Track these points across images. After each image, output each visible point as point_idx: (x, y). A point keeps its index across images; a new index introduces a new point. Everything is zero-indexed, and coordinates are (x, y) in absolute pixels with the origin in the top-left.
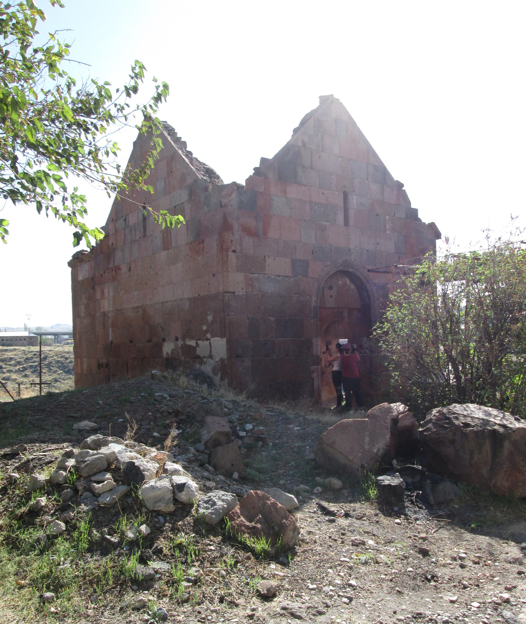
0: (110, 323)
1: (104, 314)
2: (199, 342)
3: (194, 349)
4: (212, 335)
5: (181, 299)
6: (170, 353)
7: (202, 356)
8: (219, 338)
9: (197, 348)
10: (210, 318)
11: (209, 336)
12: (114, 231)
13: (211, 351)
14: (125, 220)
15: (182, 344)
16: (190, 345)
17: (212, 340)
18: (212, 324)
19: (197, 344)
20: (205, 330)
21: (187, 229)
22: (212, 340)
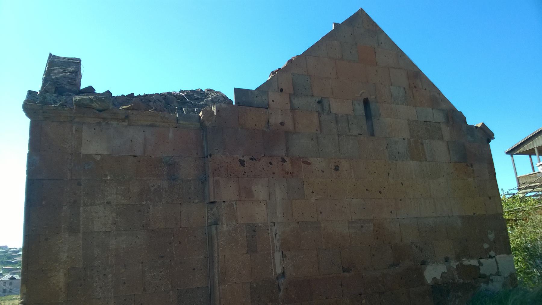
1: (253, 229)
2: (482, 260)
5: (449, 216)
6: (438, 277)
7: (488, 274)
8: (505, 255)
9: (481, 267)
10: (491, 236)
11: (492, 253)
12: (289, 108)
13: (498, 269)
14: (319, 102)
15: (457, 266)
17: (497, 257)
18: (494, 242)
19: (479, 262)
20: (487, 249)
21: (448, 149)
22: (497, 257)
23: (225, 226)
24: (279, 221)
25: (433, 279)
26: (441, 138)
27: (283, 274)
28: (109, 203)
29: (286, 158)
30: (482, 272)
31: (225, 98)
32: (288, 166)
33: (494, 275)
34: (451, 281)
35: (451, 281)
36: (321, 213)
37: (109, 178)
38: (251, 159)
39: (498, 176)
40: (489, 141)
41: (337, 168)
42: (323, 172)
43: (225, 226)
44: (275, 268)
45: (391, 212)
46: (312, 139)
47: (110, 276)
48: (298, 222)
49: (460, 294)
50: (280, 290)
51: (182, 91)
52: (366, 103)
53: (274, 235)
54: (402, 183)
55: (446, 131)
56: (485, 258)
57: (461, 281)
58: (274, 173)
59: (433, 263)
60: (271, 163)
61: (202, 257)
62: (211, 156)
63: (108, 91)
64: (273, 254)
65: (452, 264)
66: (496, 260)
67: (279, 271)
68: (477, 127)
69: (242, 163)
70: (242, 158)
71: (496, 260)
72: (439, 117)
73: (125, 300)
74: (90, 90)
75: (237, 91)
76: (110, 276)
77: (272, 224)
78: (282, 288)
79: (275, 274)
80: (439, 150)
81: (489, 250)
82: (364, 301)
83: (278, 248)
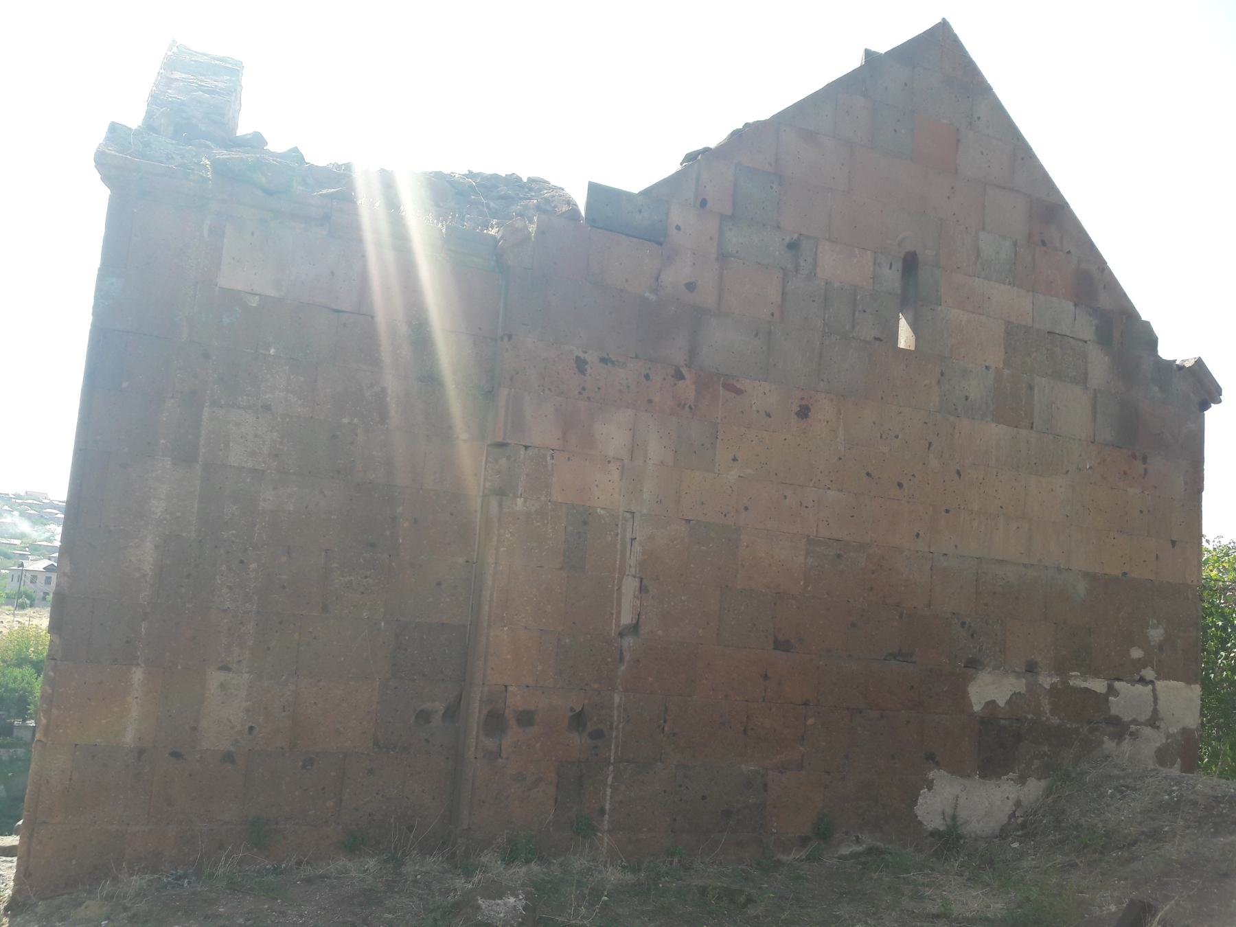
0: (632, 560)
2: (1117, 684)
3: (1101, 701)
4: (1157, 672)
5: (1058, 569)
7: (1126, 719)
8: (1181, 684)
9: (1111, 699)
10: (1156, 634)
11: (1149, 673)
13: (1155, 711)
14: (793, 246)
16: (1087, 690)
17: (1160, 684)
18: (1161, 648)
19: (1111, 690)
23: (520, 501)
24: (645, 511)
25: (988, 703)
26: (1083, 380)
27: (635, 628)
28: (267, 408)
29: (684, 371)
30: (1114, 711)
31: (569, 202)
32: (687, 389)
33: (1141, 724)
34: (1029, 717)
35: (1029, 717)
36: (746, 509)
37: (272, 351)
38: (604, 360)
39: (1206, 496)
40: (1205, 406)
41: (804, 412)
42: (769, 416)
43: (520, 501)
44: (619, 613)
45: (918, 535)
46: (757, 335)
47: (253, 566)
48: (689, 521)
49: (1046, 749)
50: (621, 659)
51: (471, 175)
52: (910, 264)
53: (628, 540)
54: (958, 473)
55: (1099, 365)
56: (1127, 682)
57: (1056, 721)
58: (650, 401)
59: (996, 668)
60: (647, 377)
61: (461, 560)
62: (510, 337)
63: (295, 150)
64: (621, 580)
65: (1041, 679)
66: (1154, 691)
67: (627, 618)
68: (1181, 368)
69: (581, 365)
70: (581, 355)
71: (1154, 691)
72: (1085, 328)
73: (281, 623)
74: (257, 141)
75: (597, 192)
76: (253, 566)
77: (628, 515)
78: (627, 657)
79: (618, 625)
80: (1072, 410)
81: (1143, 663)
82: (810, 721)
83: (633, 570)
